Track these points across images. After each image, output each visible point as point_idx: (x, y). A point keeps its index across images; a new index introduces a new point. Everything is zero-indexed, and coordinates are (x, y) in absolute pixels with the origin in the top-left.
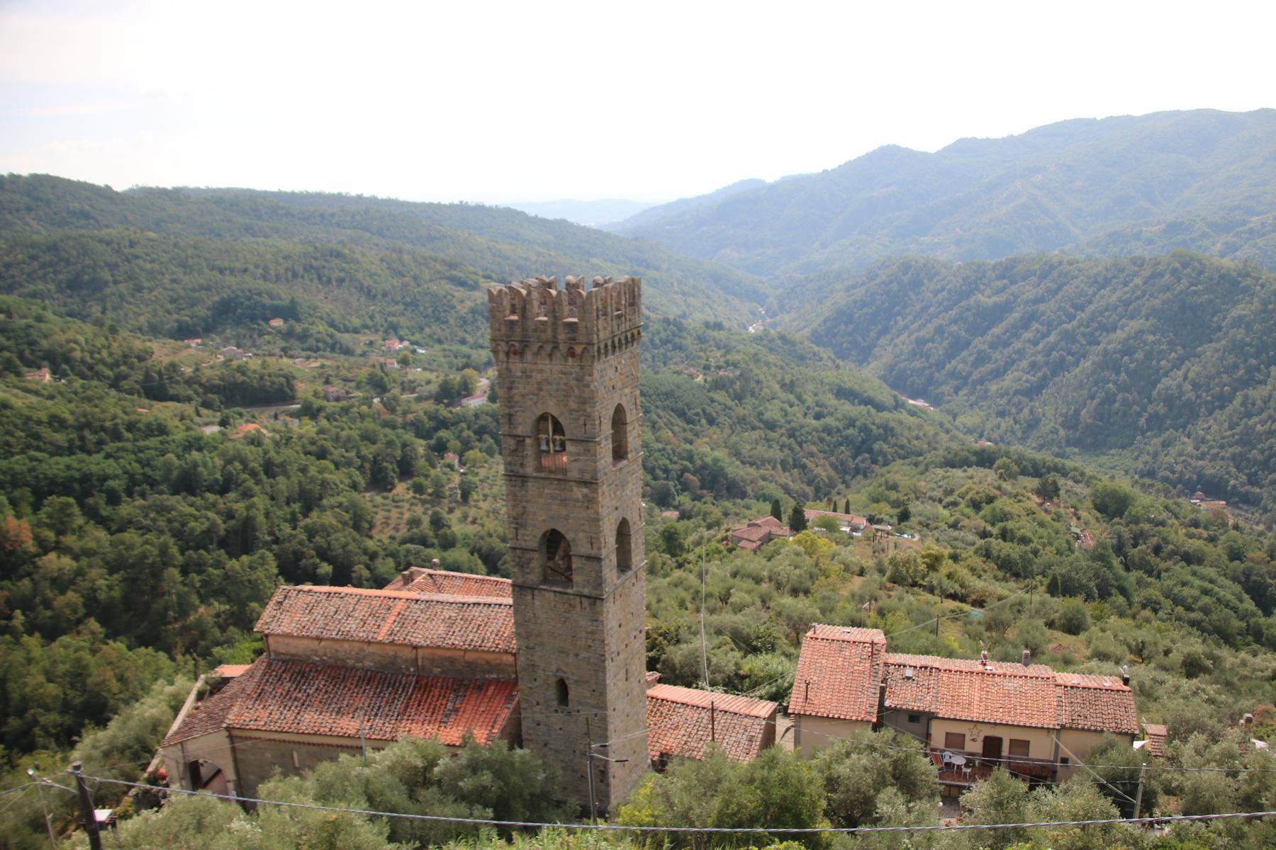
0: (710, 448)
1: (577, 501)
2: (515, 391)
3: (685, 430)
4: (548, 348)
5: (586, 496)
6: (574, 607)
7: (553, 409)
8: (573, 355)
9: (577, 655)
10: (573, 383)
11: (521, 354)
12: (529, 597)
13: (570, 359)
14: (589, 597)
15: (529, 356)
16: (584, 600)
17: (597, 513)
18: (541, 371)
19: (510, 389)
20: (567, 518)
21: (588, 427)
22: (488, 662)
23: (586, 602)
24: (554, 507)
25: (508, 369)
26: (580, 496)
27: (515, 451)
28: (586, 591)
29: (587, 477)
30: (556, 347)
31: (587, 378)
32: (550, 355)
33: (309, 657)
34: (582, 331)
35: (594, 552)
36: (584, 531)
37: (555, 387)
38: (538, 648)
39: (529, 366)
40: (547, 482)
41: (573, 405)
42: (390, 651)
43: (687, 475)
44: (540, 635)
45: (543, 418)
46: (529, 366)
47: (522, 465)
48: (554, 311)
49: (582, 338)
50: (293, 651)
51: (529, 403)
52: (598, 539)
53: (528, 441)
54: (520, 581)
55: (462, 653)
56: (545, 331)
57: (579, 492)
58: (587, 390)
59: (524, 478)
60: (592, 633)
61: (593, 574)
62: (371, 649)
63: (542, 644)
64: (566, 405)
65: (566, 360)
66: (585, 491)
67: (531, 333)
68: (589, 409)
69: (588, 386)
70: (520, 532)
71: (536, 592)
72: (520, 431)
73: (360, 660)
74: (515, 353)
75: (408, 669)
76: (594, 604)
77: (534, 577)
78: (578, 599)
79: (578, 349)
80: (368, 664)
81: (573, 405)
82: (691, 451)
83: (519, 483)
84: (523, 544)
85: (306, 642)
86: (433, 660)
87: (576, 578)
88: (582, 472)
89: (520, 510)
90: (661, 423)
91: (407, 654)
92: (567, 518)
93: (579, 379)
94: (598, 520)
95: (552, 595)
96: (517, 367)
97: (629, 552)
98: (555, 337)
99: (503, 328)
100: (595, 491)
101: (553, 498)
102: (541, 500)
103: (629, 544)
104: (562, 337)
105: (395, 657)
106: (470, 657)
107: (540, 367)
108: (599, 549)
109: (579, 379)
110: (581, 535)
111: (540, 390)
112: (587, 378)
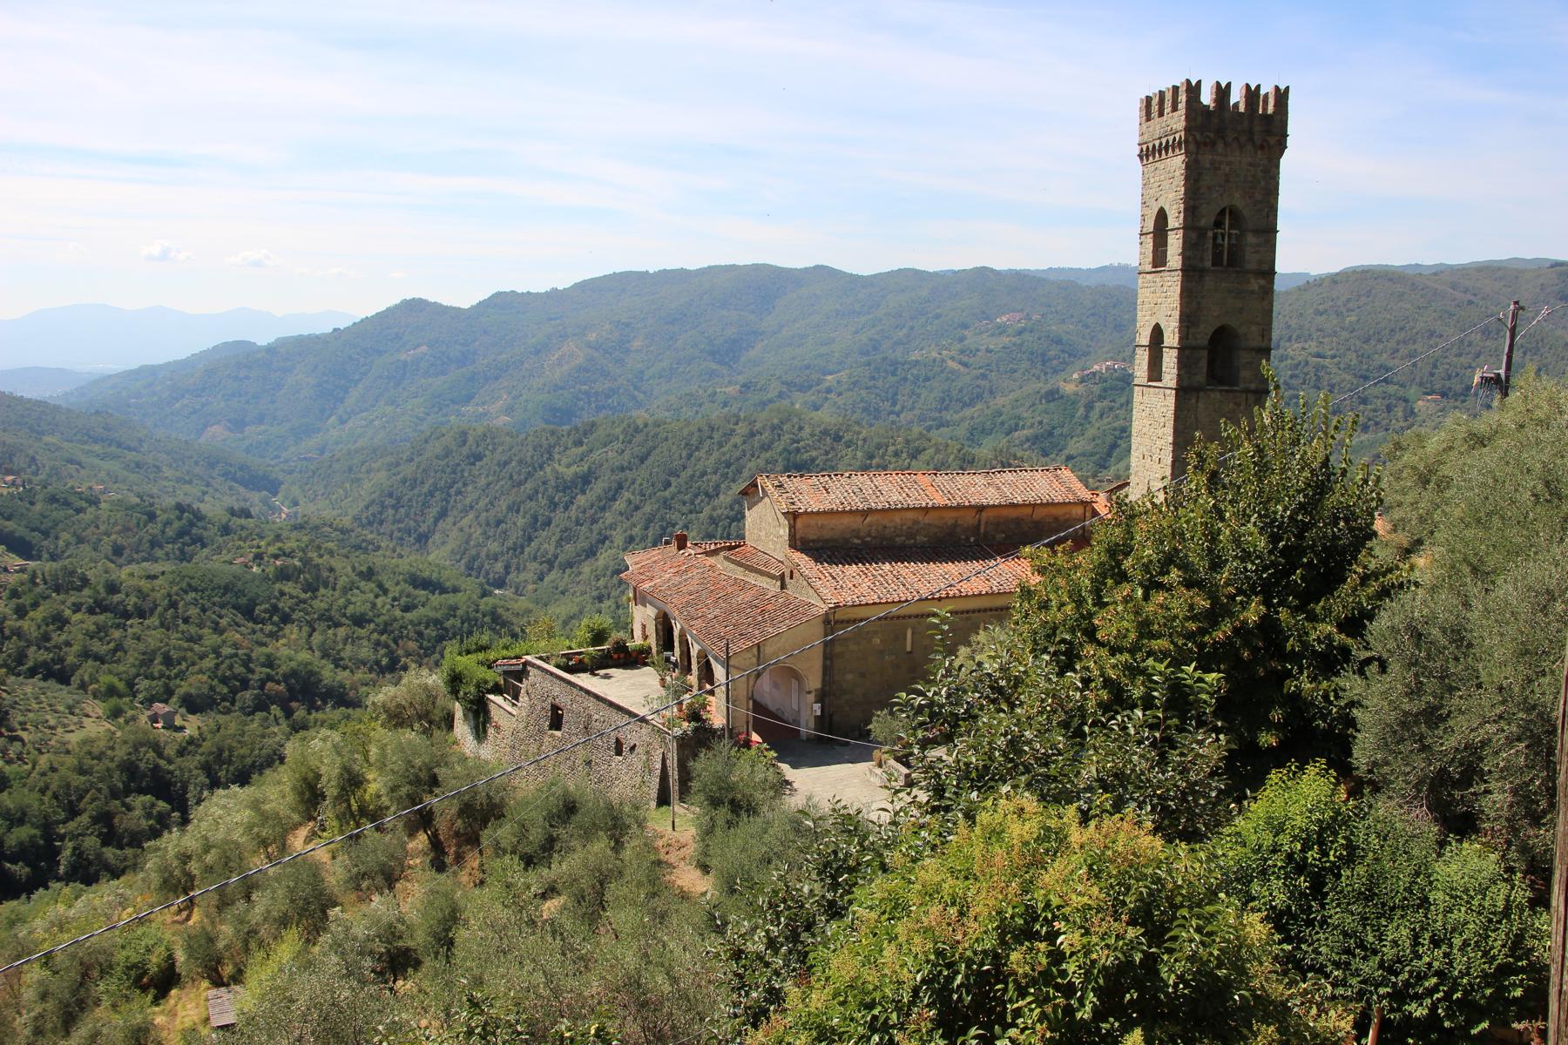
0: (292, 649)
1: (1252, 292)
3: (254, 632)
4: (1243, 139)
5: (1261, 287)
7: (1238, 200)
8: (1262, 147)
14: (1255, 392)
15: (1220, 147)
18: (1230, 163)
19: (1196, 181)
22: (1056, 519)
23: (1251, 398)
25: (1196, 161)
28: (1253, 386)
29: (1265, 267)
30: (1251, 140)
32: (1241, 147)
33: (847, 541)
41: (1258, 197)
42: (949, 517)
43: (269, 685)
45: (1222, 212)
46: (1219, 158)
47: (1202, 259)
50: (827, 534)
54: (1185, 384)
55: (1029, 510)
57: (1255, 284)
59: (1203, 271)
62: (928, 519)
66: (1262, 282)
72: (1203, 222)
73: (911, 536)
74: (1205, 144)
75: (967, 539)
79: (1272, 140)
80: (921, 539)
81: (1258, 197)
82: (268, 656)
84: (1194, 343)
85: (846, 520)
86: (998, 524)
90: (223, 622)
91: (969, 519)
96: (1206, 159)
99: (1199, 119)
100: (1272, 282)
104: (1257, 128)
105: (955, 525)
106: (1039, 514)
110: (1254, 328)
111: (1228, 181)
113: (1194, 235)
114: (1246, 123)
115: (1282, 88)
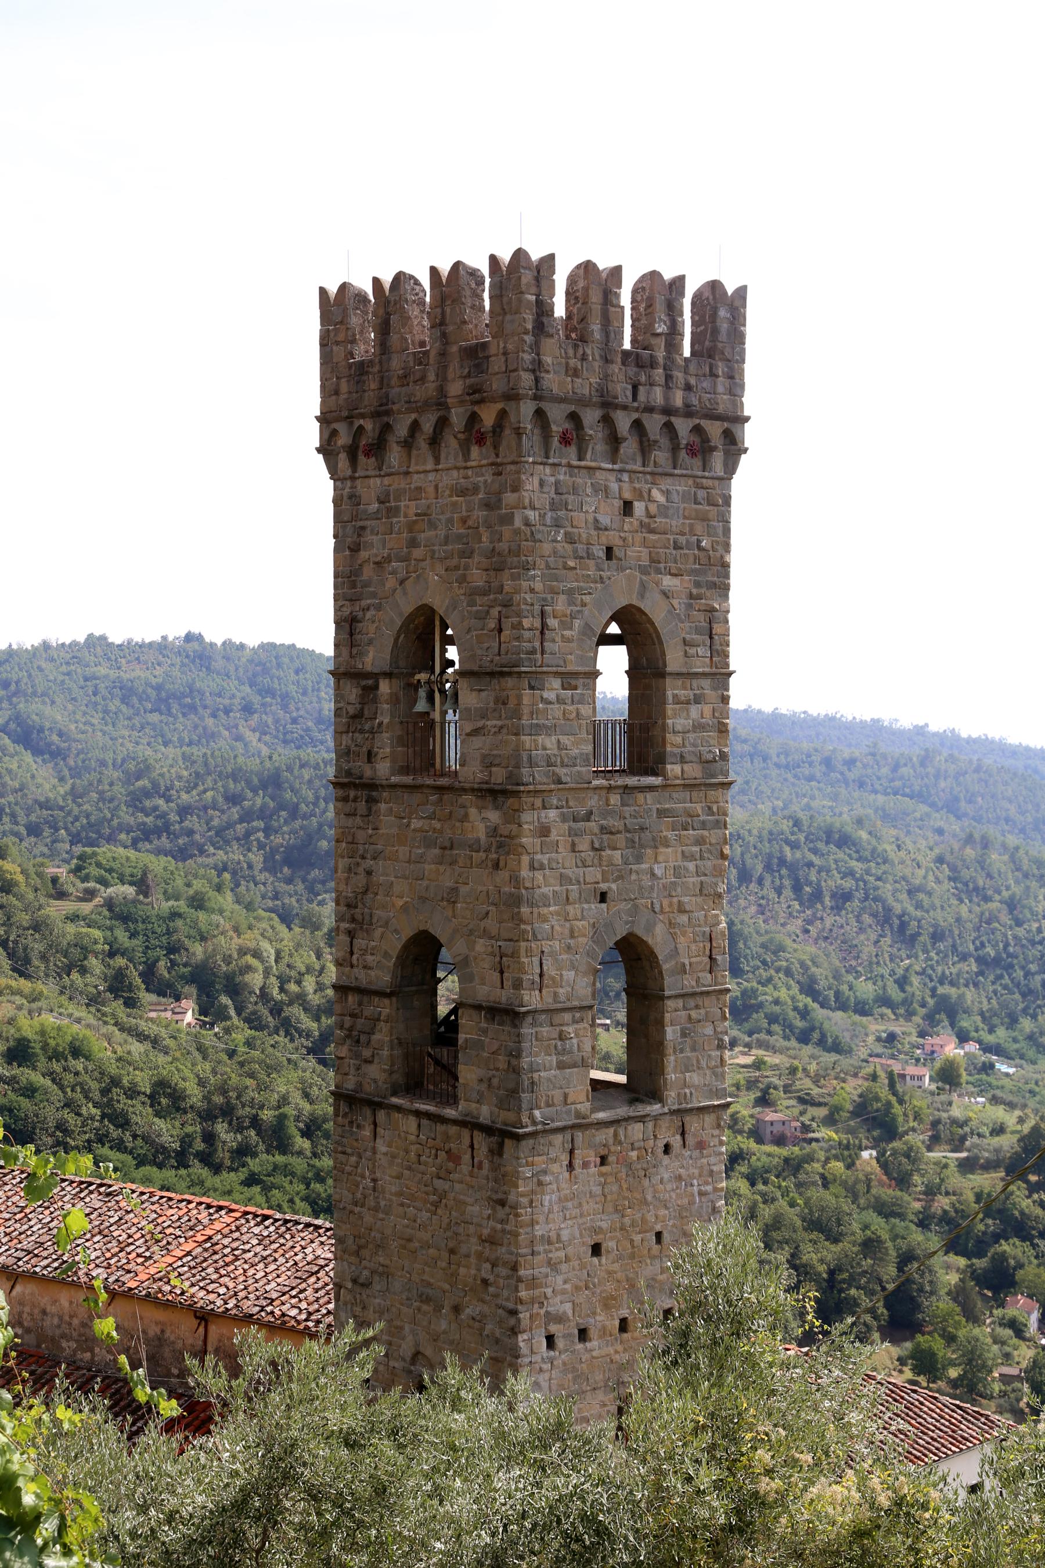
1: (475, 846)
2: (364, 554)
6: (453, 1157)
9: (457, 1309)
10: (480, 514)
11: (378, 448)
12: (367, 1132)
13: (475, 451)
14: (487, 1130)
15: (395, 456)
16: (479, 1137)
17: (515, 880)
19: (355, 549)
20: (452, 897)
21: (506, 633)
24: (429, 868)
26: (480, 832)
27: (358, 716)
28: (485, 1113)
29: (499, 776)
31: (509, 497)
34: (497, 364)
35: (503, 996)
36: (486, 934)
37: (442, 533)
38: (377, 1286)
39: (398, 483)
40: (417, 797)
41: (478, 577)
44: (380, 1246)
47: (370, 756)
48: (442, 323)
49: (497, 385)
51: (391, 583)
52: (515, 954)
53: (385, 687)
54: (350, 1085)
56: (423, 379)
57: (480, 821)
58: (506, 531)
60: (492, 1241)
61: (502, 1061)
63: (386, 1274)
64: (462, 580)
65: (467, 456)
66: (494, 816)
67: (394, 392)
68: (508, 585)
69: (508, 519)
70: (359, 943)
71: (381, 1115)
76: (501, 1145)
77: (376, 1075)
78: (466, 1133)
79: (488, 416)
83: (362, 806)
87: (468, 1074)
88: (488, 763)
89: (361, 880)
92: (452, 897)
93: (491, 505)
94: (515, 901)
95: (412, 1122)
96: (371, 488)
97: (659, 1047)
98: (442, 391)
100: (513, 817)
101: (429, 843)
102: (403, 851)
103: (660, 1024)
107: (417, 480)
108: (518, 985)
109: (491, 505)
110: (481, 946)
111: (413, 543)
112: (509, 497)
113: (353, 693)
114: (431, 376)
115: (535, 255)
